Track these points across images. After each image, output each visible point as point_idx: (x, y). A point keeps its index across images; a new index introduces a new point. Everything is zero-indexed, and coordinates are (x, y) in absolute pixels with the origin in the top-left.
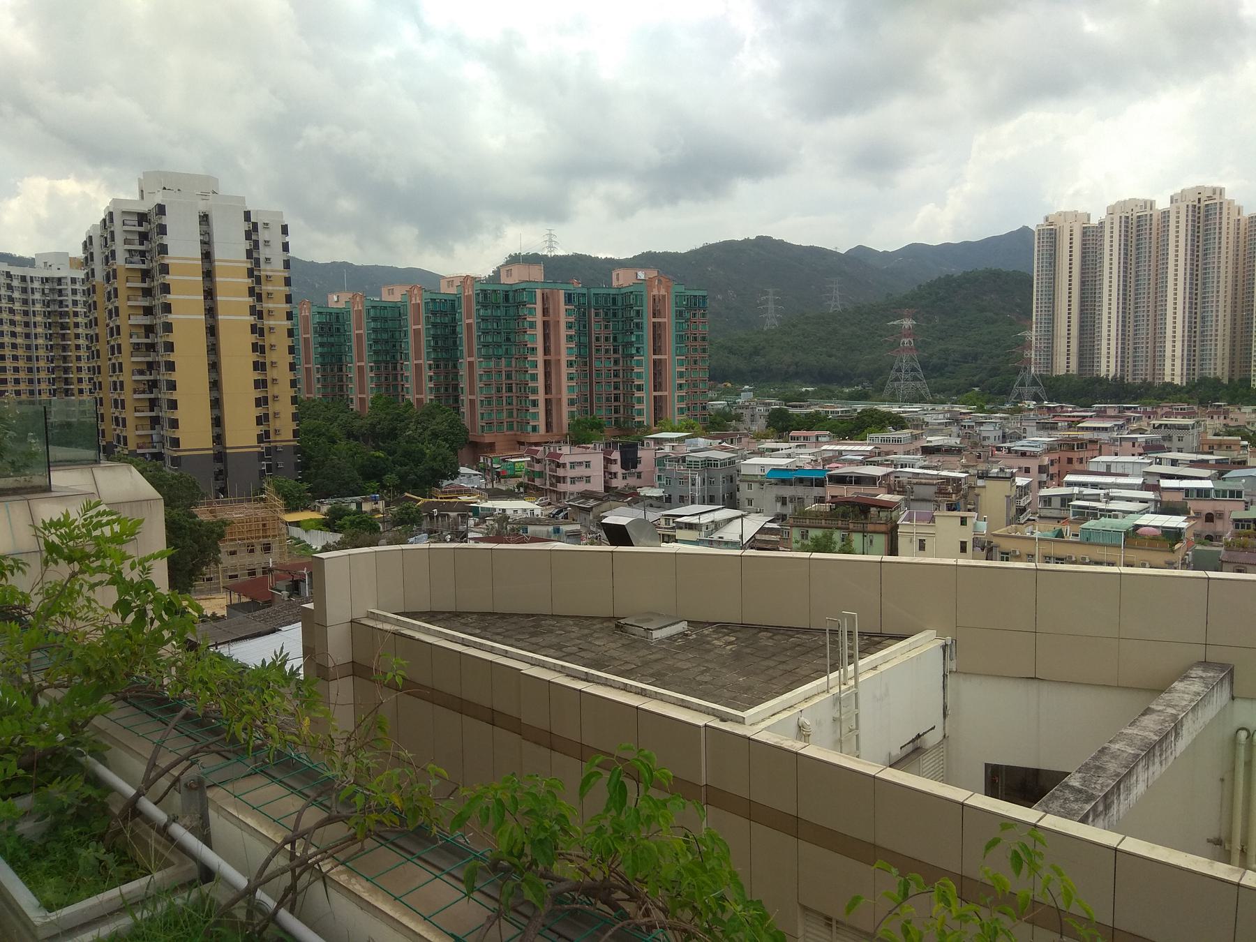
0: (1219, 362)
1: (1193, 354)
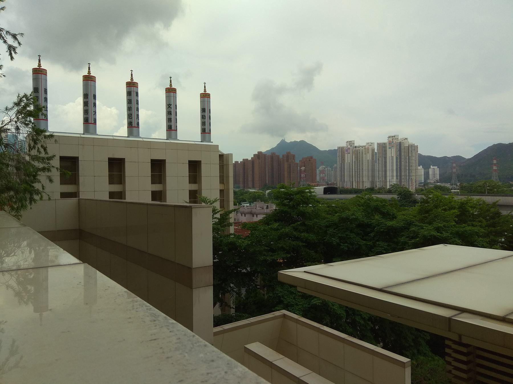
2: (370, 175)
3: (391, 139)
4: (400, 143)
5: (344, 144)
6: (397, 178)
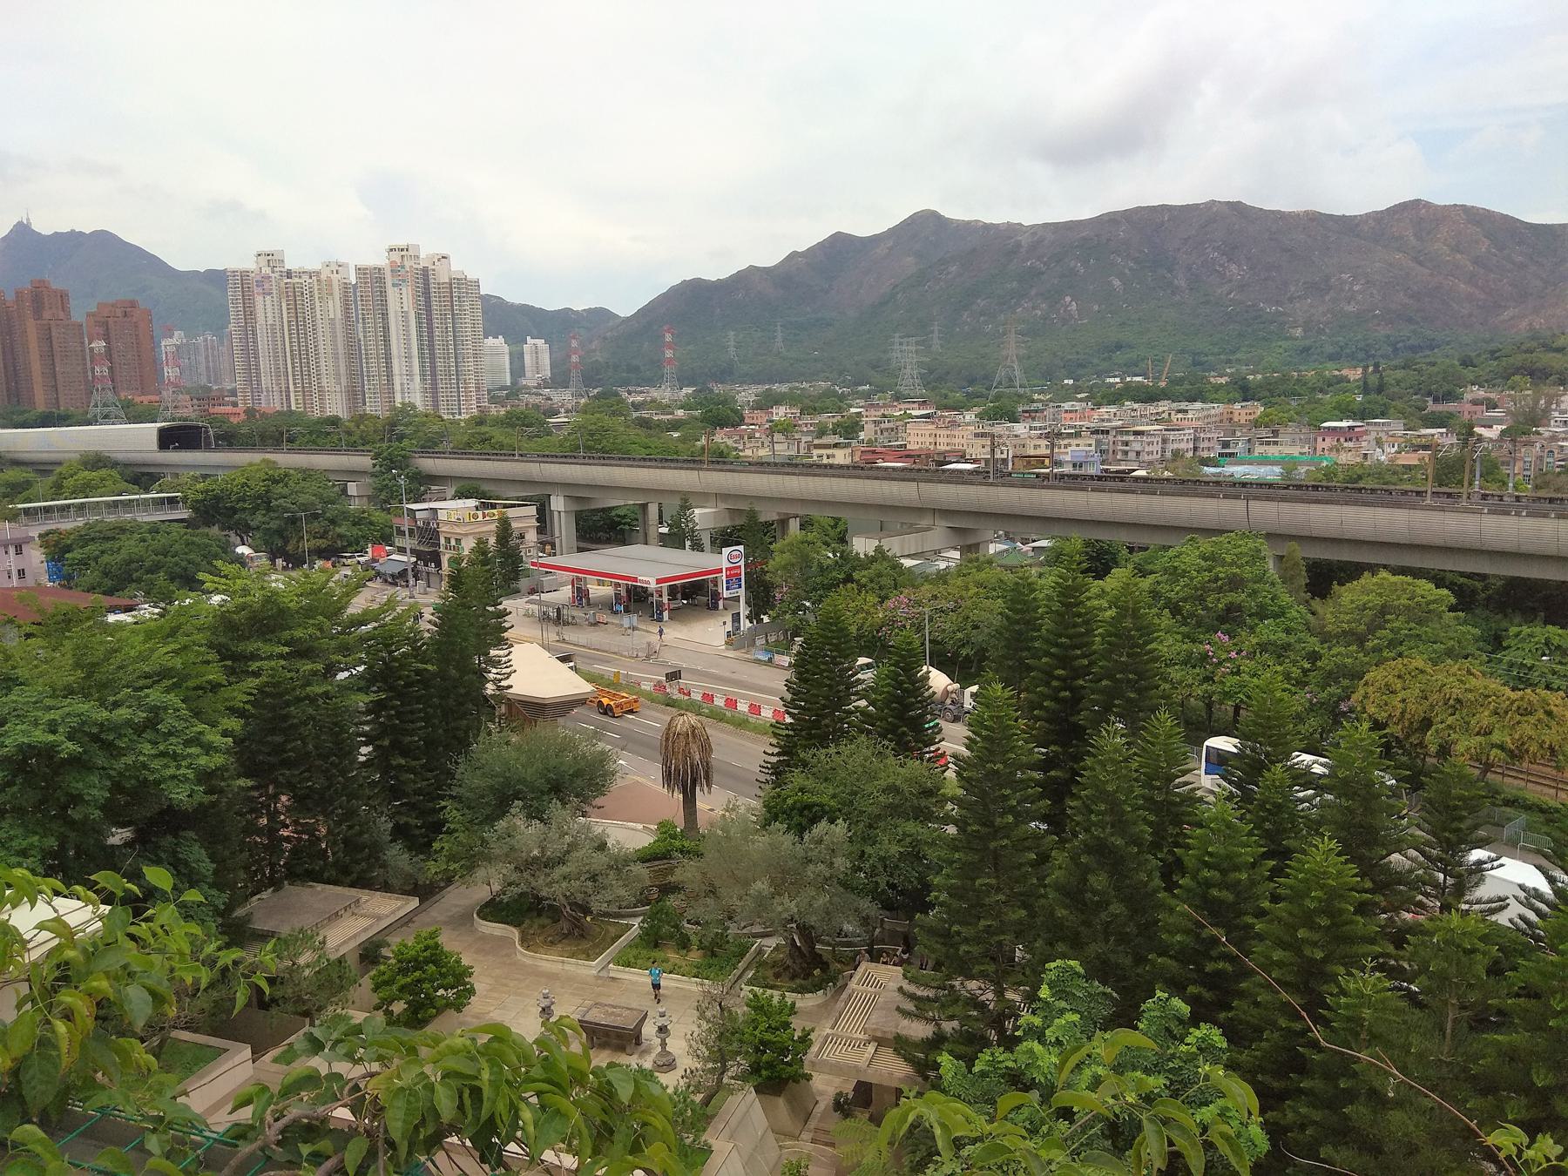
2: (343, 369)
3: (396, 257)
4: (425, 270)
5: (249, 264)
6: (423, 380)
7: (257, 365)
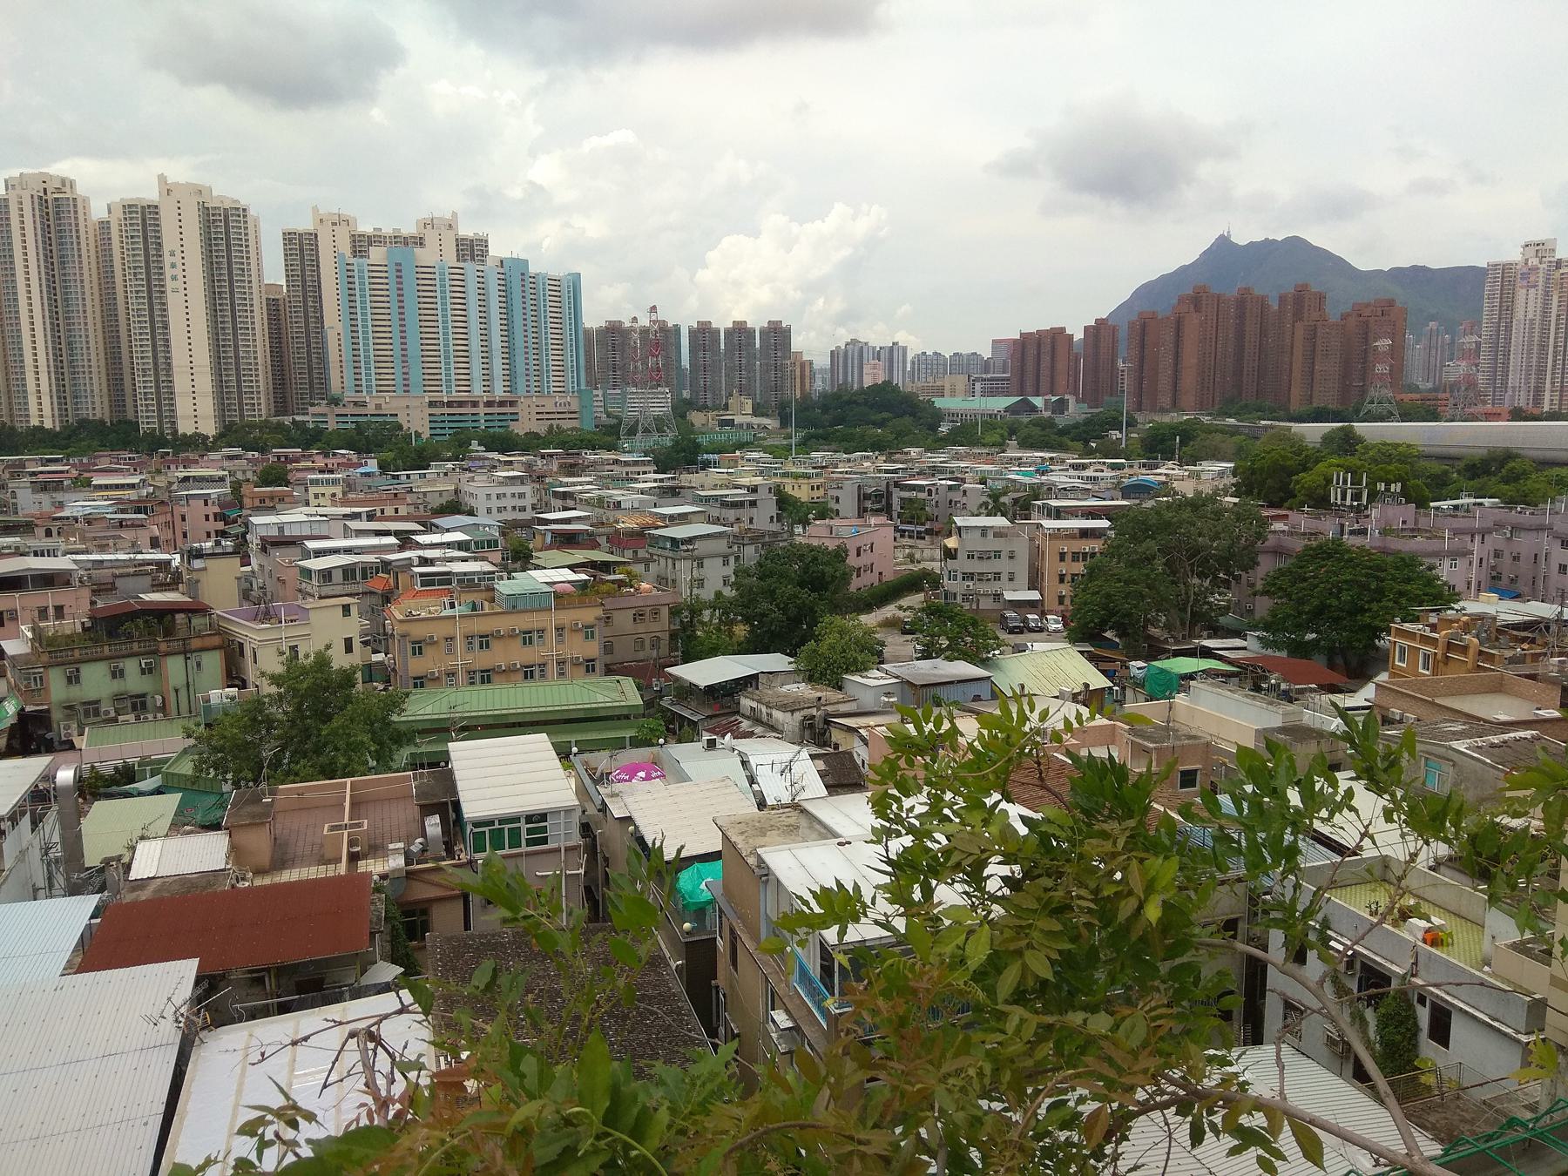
0: (97, 399)
1: (65, 391)
5: (1513, 254)
7: (1506, 365)
